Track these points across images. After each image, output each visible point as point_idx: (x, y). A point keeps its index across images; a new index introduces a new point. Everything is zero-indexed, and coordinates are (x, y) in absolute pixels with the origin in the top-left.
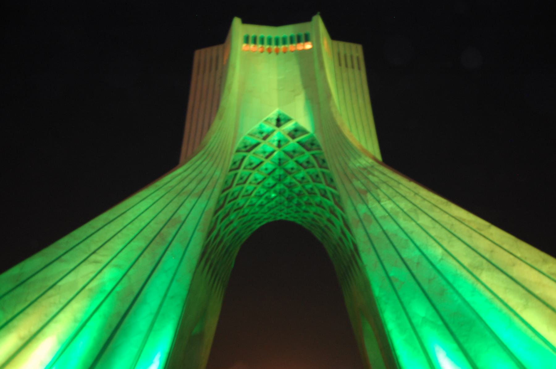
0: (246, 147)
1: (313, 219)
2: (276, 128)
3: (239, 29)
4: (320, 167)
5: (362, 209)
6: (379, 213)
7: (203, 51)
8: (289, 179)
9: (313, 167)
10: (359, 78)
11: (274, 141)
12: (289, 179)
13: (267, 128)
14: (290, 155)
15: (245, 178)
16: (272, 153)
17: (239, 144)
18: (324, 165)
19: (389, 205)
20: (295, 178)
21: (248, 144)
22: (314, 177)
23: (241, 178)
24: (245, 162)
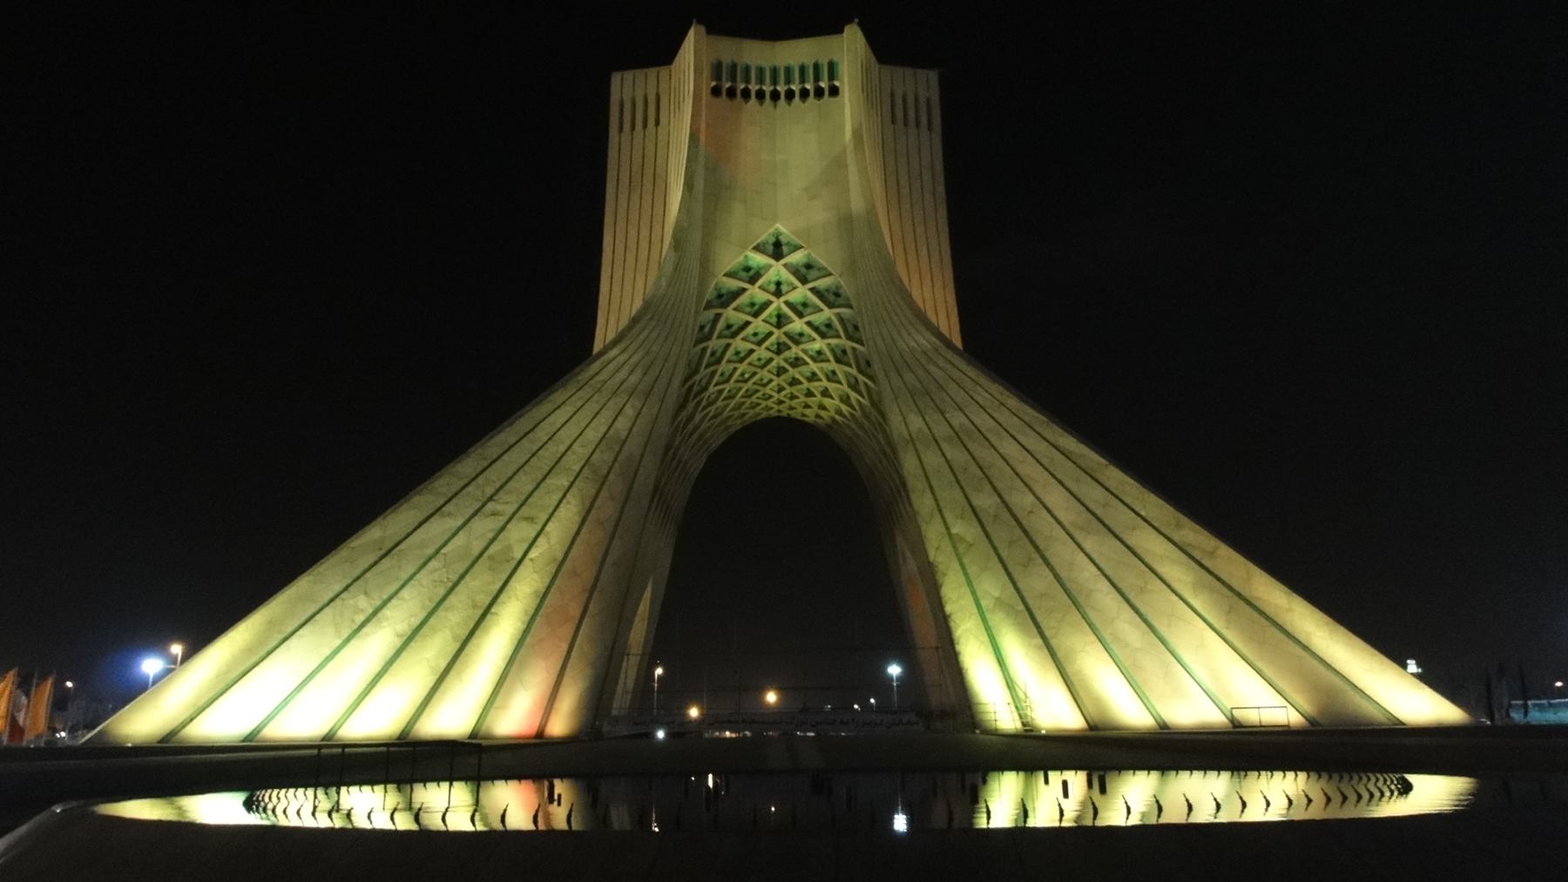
0: (720, 296)
1: (834, 420)
2: (772, 261)
4: (850, 338)
6: (942, 430)
7: (628, 75)
8: (795, 351)
9: (838, 336)
12: (795, 351)
13: (758, 259)
14: (800, 310)
16: (767, 304)
17: (710, 293)
18: (857, 335)
19: (958, 420)
20: (805, 352)
22: (839, 353)
23: (713, 354)
24: (721, 325)
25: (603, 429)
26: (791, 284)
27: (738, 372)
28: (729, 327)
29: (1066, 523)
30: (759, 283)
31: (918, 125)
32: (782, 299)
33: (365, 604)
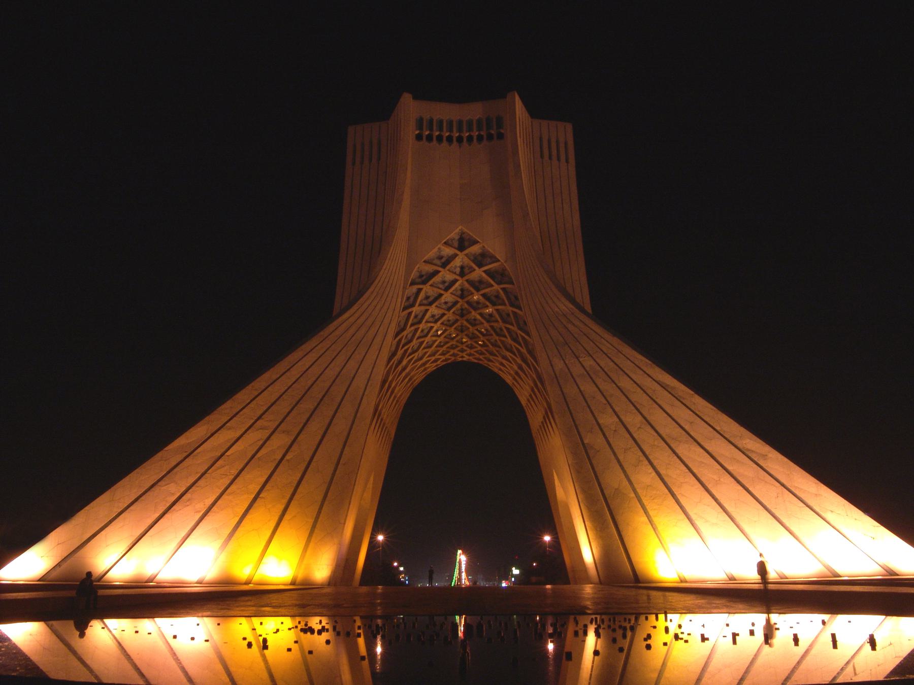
0: (421, 276)
2: (458, 252)
3: (410, 109)
4: (512, 305)
5: (559, 365)
6: (577, 370)
9: (505, 305)
10: (565, 174)
11: (456, 267)
13: (448, 251)
14: (477, 285)
15: (419, 317)
16: (454, 282)
17: (414, 274)
20: (481, 314)
21: (423, 273)
23: (416, 316)
24: (422, 295)
25: (338, 370)
26: (471, 267)
27: (434, 329)
28: (427, 298)
29: (664, 436)
30: (448, 268)
31: (559, 160)
32: (466, 278)
33: (173, 489)
